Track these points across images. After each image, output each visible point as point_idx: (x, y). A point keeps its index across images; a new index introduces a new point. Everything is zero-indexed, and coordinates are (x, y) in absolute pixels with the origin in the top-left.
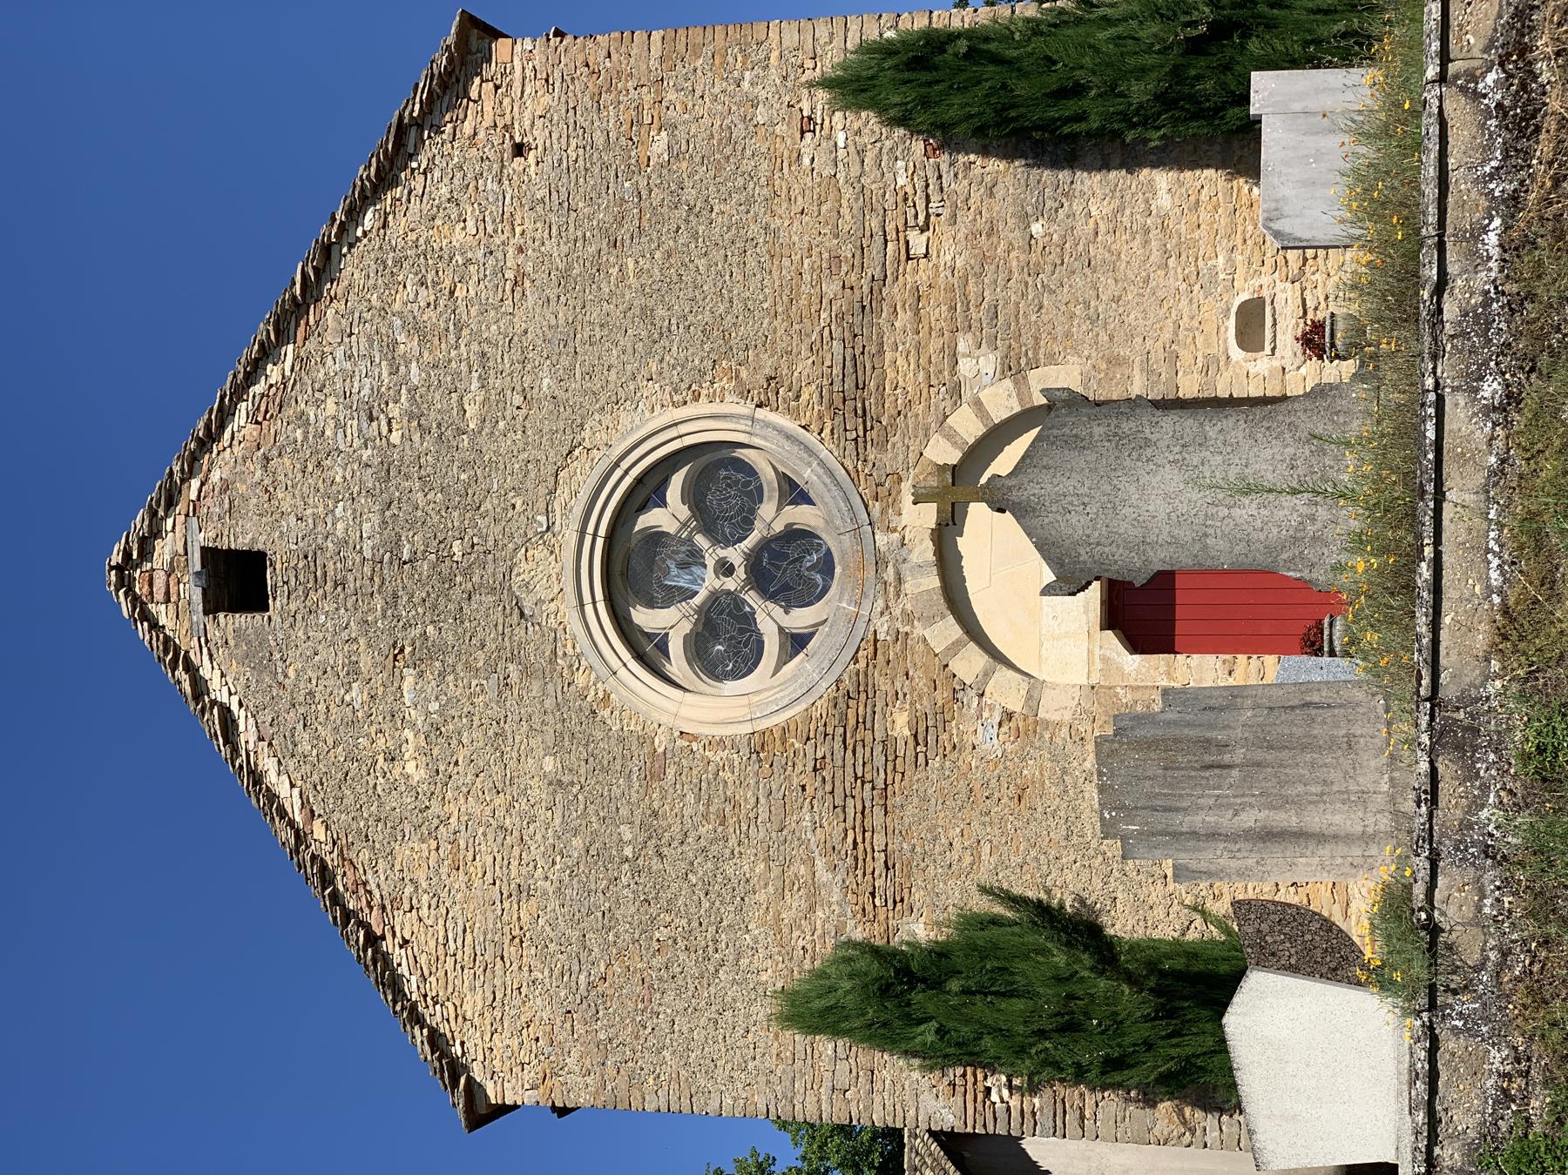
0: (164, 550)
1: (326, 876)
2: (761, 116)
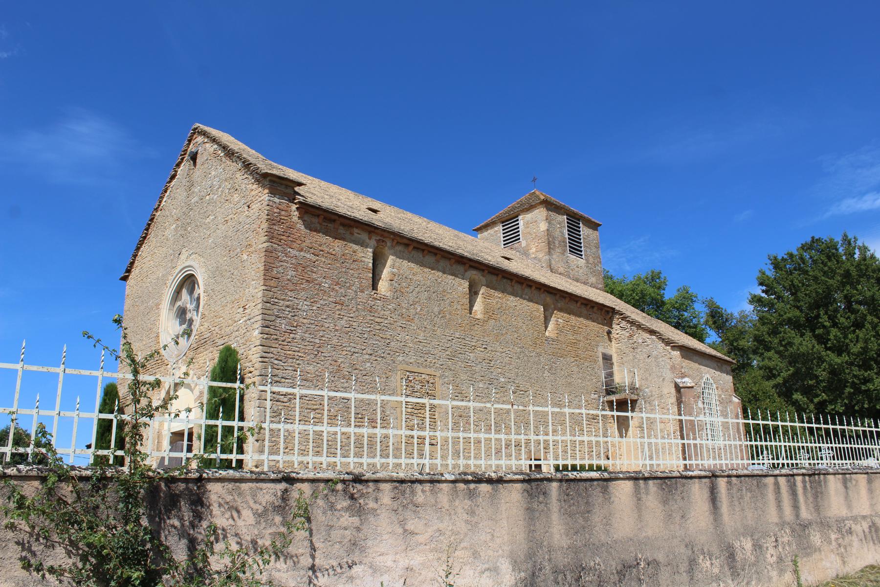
0: (200, 139)
1: (152, 220)
2: (247, 290)
